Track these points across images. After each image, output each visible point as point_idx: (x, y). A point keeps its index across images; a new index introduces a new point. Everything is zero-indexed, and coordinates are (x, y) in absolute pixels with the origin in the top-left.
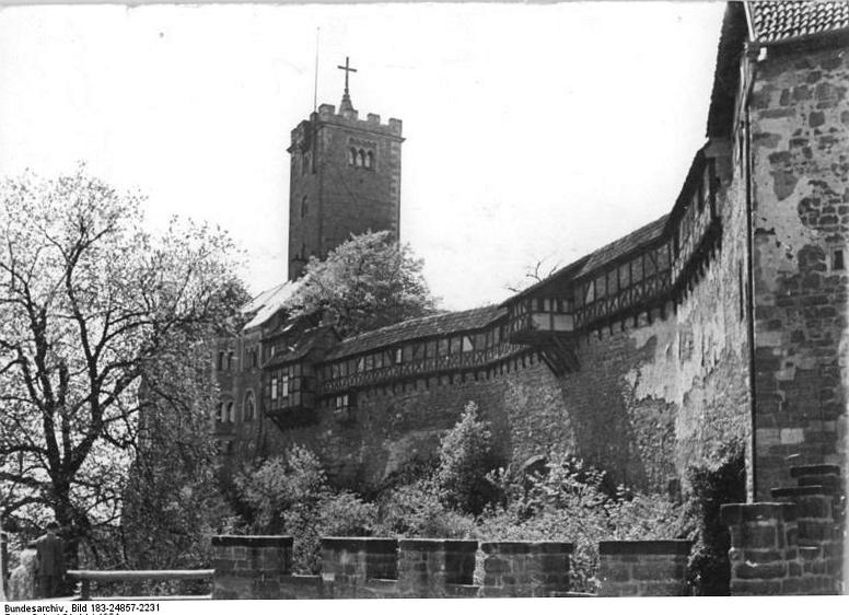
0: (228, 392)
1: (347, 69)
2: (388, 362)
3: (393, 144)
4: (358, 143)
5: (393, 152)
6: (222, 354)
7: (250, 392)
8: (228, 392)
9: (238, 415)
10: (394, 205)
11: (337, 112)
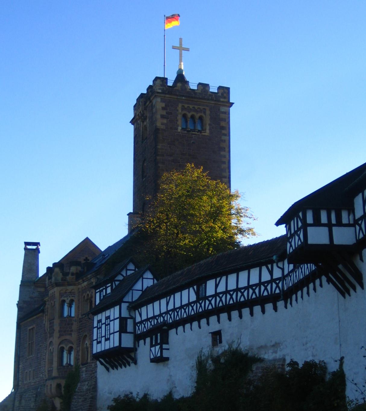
0: (68, 337)
1: (181, 48)
2: (193, 298)
3: (223, 109)
4: (189, 110)
5: (222, 116)
6: (64, 301)
7: (86, 336)
8: (68, 337)
9: (76, 359)
10: (224, 163)
11: (170, 84)
